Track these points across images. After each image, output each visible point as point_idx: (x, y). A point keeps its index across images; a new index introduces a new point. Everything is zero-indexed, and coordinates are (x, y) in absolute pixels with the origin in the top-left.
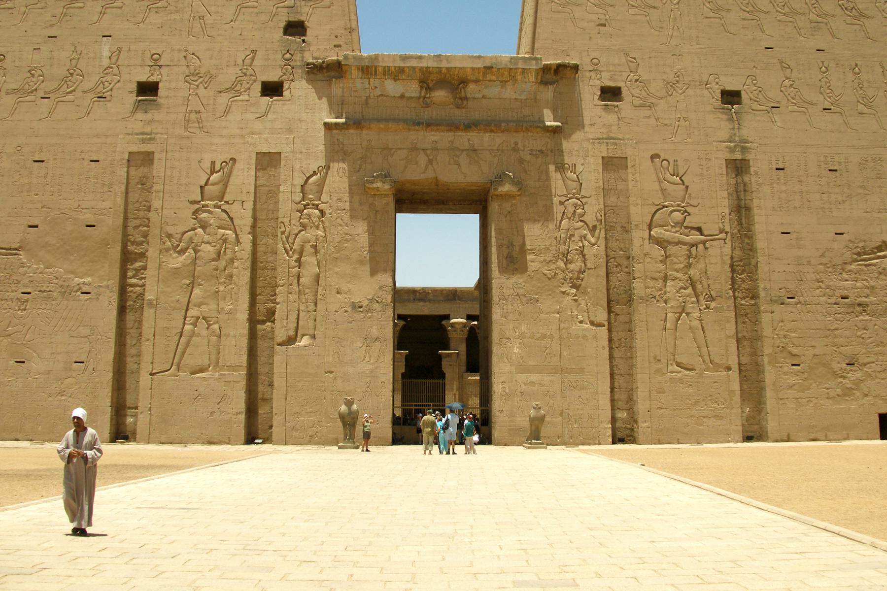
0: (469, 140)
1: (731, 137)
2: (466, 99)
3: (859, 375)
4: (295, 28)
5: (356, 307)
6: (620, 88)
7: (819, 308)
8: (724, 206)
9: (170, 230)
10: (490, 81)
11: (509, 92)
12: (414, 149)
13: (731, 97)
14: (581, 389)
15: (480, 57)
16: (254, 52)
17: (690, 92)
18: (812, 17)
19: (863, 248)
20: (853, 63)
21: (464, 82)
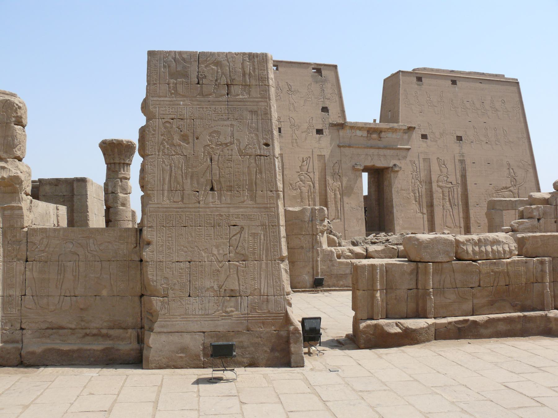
4: (325, 110)
5: (352, 208)
6: (426, 135)
9: (291, 182)
11: (394, 136)
12: (367, 155)
13: (460, 138)
16: (312, 118)
21: (381, 132)
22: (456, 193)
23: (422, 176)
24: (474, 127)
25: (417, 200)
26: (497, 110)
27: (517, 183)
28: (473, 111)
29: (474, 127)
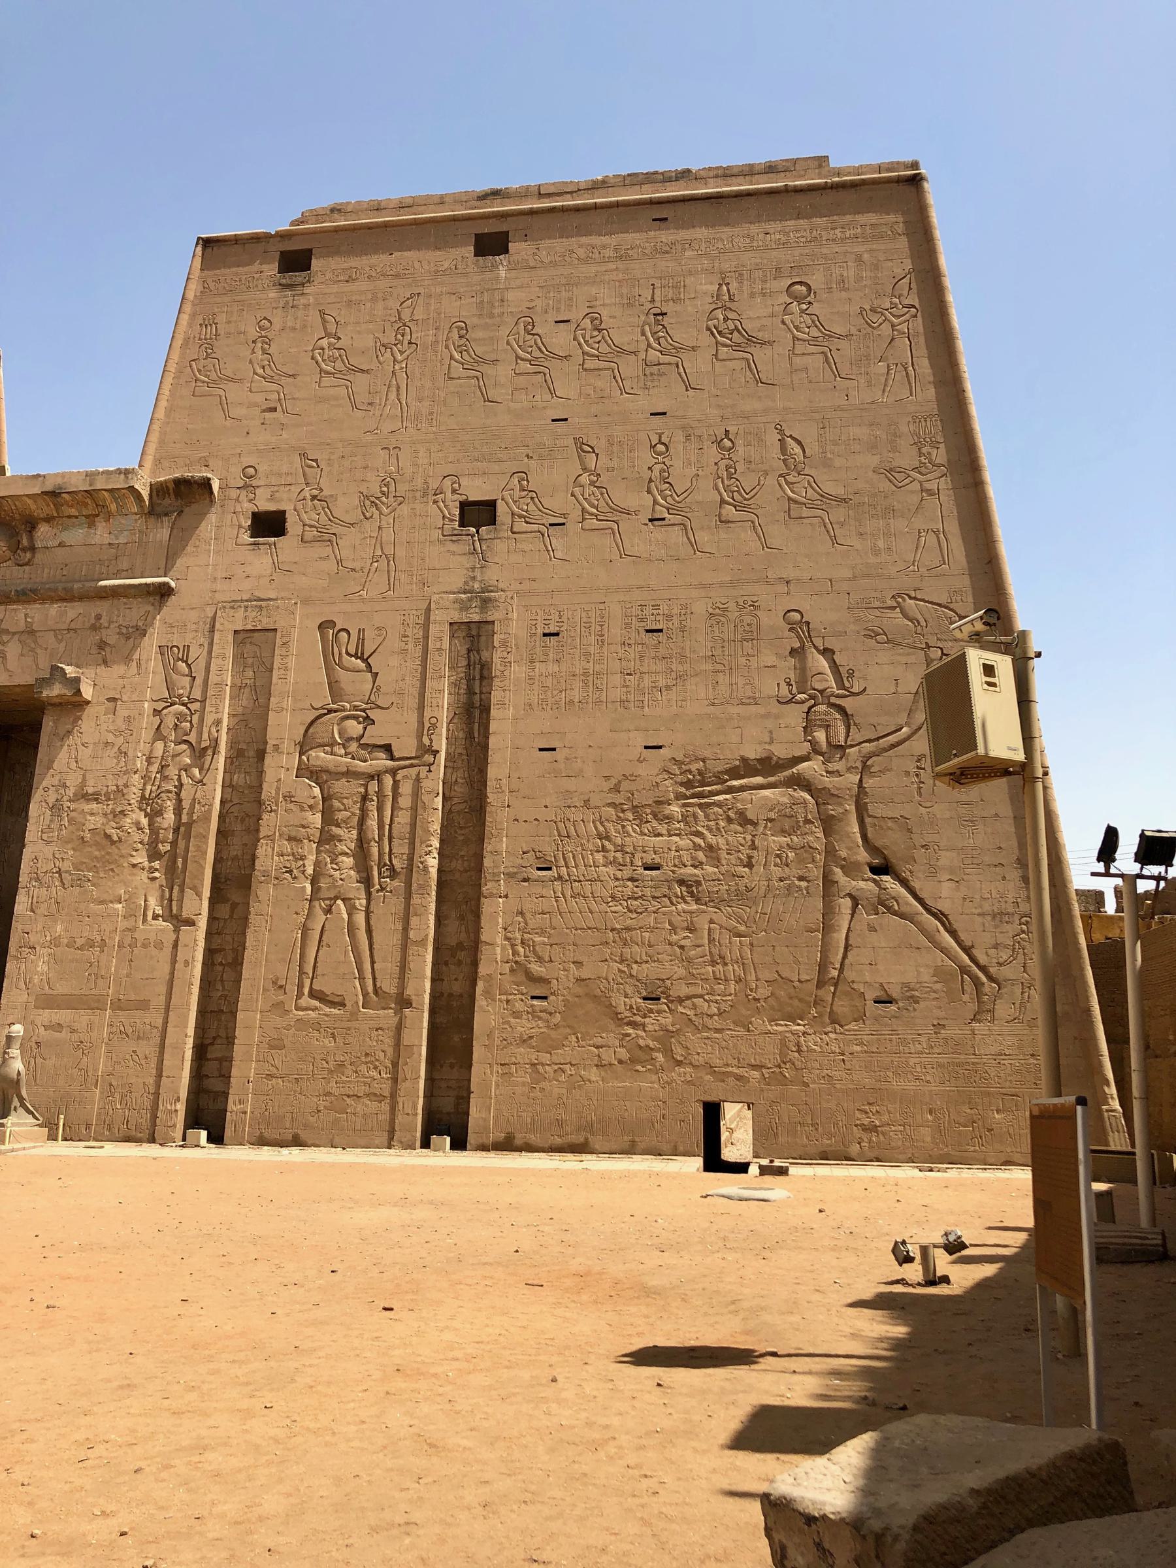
0: (26, 616)
1: (466, 583)
2: (33, 549)
3: (667, 1020)
7: (597, 887)
8: (443, 704)
10: (70, 517)
11: (101, 534)
13: (477, 514)
14: (139, 1038)
15: (38, 475)
17: (404, 510)
18: (654, 355)
19: (700, 772)
20: (720, 433)
21: (31, 524)
22: (405, 801)
23: (209, 719)
24: (581, 447)
25: (164, 848)
26: (751, 340)
27: (856, 736)
28: (591, 364)
29: (580, 445)
